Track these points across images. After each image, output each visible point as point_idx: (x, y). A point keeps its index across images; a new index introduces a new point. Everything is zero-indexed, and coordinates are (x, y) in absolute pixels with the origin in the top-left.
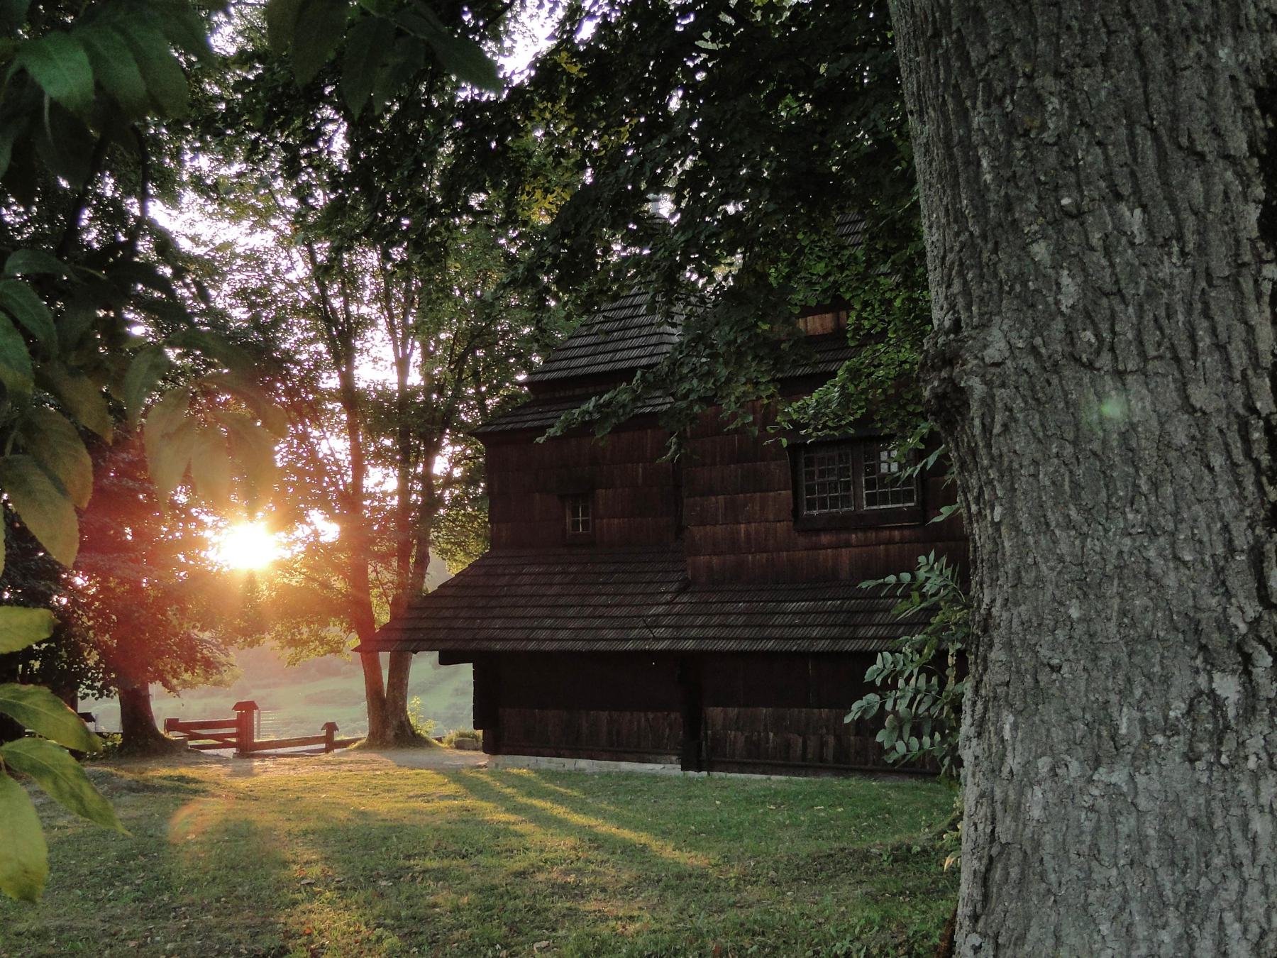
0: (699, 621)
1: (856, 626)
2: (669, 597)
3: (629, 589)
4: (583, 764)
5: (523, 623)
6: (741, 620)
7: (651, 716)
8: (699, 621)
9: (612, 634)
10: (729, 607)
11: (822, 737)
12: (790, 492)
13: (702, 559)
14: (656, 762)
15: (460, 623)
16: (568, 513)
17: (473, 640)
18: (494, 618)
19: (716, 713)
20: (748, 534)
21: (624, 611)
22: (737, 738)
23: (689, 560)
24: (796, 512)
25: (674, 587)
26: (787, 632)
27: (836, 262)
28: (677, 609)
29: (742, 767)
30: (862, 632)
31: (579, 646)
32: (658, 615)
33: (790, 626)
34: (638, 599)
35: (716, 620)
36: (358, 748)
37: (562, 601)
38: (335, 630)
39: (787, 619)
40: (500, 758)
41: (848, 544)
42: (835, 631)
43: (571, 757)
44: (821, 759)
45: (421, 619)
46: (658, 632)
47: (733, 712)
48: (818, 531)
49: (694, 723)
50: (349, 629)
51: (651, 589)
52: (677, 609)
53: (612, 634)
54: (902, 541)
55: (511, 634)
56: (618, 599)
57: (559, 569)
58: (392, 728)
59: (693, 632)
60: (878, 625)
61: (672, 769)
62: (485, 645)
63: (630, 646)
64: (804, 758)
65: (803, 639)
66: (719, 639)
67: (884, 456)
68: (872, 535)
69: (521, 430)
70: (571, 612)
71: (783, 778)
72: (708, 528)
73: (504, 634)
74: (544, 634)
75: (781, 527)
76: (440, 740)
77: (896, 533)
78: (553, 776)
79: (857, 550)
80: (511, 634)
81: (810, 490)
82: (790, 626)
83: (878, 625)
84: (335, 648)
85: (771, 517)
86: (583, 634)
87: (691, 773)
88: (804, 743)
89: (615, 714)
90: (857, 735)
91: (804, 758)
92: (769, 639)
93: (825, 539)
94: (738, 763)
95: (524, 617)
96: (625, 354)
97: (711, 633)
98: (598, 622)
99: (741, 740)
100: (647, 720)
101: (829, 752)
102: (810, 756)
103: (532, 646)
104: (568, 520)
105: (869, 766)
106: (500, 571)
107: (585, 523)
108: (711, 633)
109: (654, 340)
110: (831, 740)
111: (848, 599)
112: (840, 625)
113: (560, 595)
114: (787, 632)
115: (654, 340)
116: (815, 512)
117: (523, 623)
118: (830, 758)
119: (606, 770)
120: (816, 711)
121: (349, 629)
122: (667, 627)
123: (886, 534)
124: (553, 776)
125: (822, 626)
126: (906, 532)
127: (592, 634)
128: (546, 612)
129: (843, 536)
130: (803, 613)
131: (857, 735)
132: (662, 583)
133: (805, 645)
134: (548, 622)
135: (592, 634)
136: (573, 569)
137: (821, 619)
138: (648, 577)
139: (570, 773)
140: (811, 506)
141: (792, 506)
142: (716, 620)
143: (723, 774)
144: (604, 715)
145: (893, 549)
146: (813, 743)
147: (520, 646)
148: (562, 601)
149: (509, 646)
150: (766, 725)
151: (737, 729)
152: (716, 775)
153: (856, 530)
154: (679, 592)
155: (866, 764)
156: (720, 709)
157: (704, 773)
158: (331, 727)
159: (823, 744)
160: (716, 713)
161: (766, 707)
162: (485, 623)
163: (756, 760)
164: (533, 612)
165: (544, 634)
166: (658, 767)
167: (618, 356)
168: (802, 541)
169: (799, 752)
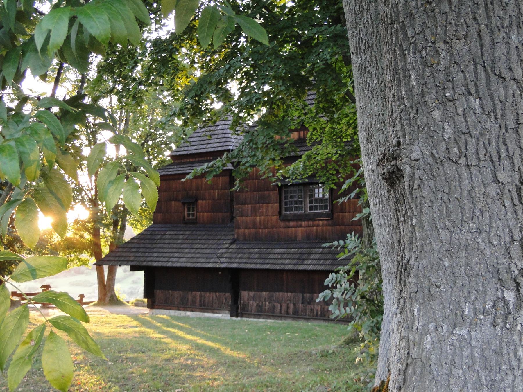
0: (240, 256)
1: (304, 259)
2: (227, 246)
3: (211, 242)
4: (189, 313)
5: (167, 255)
6: (257, 256)
7: (218, 294)
8: (240, 256)
9: (203, 260)
10: (252, 251)
11: (288, 304)
12: (278, 204)
13: (241, 231)
14: (219, 313)
15: (139, 254)
16: (186, 209)
17: (145, 261)
18: (154, 252)
19: (244, 294)
20: (260, 221)
21: (208, 251)
22: (253, 304)
23: (236, 231)
24: (280, 213)
25: (229, 242)
26: (275, 261)
27: (303, 112)
28: (230, 250)
29: (255, 316)
30: (306, 262)
31: (189, 265)
32: (223, 253)
33: (277, 259)
34: (214, 246)
35: (246, 256)
36: (94, 305)
37: (182, 246)
38: (85, 256)
39: (275, 256)
40: (155, 311)
41: (301, 226)
42: (295, 261)
43: (184, 310)
44: (287, 313)
45: (123, 252)
46: (222, 260)
47: (252, 293)
48: (289, 220)
49: (236, 298)
50: (91, 255)
51: (221, 242)
52: (230, 250)
53: (203, 260)
54: (323, 226)
55: (160, 259)
56: (206, 246)
57: (181, 233)
58: (108, 297)
59: (237, 260)
60: (312, 259)
61: (224, 316)
62: (150, 264)
63: (210, 265)
64: (280, 313)
65: (282, 264)
66: (247, 263)
67: (317, 191)
68: (311, 223)
69: (167, 175)
70: (186, 251)
71: (273, 321)
72: (244, 218)
73: (158, 259)
74: (175, 260)
75: (274, 218)
76: (128, 302)
77: (321, 222)
78: (177, 318)
79: (305, 229)
80: (160, 259)
81: (286, 204)
82: (277, 259)
83: (312, 259)
84: (84, 263)
85: (270, 214)
86: (191, 260)
87: (234, 318)
88: (281, 306)
89: (203, 293)
90: (302, 303)
91: (280, 313)
92: (268, 264)
93: (292, 224)
95: (166, 253)
96: (212, 145)
97: (244, 261)
98: (198, 255)
99: (255, 305)
100: (216, 295)
101: (291, 311)
102: (283, 312)
103: (169, 264)
104: (186, 213)
105: (307, 317)
106: (157, 233)
107: (193, 215)
108: (244, 261)
109: (224, 140)
110: (292, 306)
111: (300, 248)
112: (297, 259)
113: (181, 244)
114: (275, 261)
115: (224, 140)
116: (288, 213)
117: (167, 255)
118: (291, 313)
119: (198, 316)
120: (286, 293)
121: (91, 255)
122: (226, 258)
123: (317, 222)
124: (177, 318)
125: (290, 259)
126: (325, 222)
127: (194, 260)
128: (175, 250)
129: (299, 223)
130: (282, 254)
131: (302, 303)
132: (225, 240)
133: (282, 267)
134: (176, 255)
135: (194, 260)
136: (187, 233)
137: (289, 256)
138: (219, 237)
139: (184, 317)
140: (286, 210)
141: (278, 210)
142: (246, 256)
143: (247, 319)
144: (198, 293)
145: (319, 228)
146: (284, 306)
147: (165, 264)
148: (182, 246)
149: (159, 264)
150: (265, 299)
151: (254, 301)
152: (245, 319)
153: (304, 220)
154: (232, 244)
155: (306, 315)
156: (247, 292)
157: (239, 318)
158: (82, 296)
159: (288, 308)
160: (244, 294)
161: (266, 291)
162: (150, 254)
163: (260, 313)
164: (171, 250)
165: (175, 260)
167: (209, 146)
168: (282, 224)
169: (278, 311)
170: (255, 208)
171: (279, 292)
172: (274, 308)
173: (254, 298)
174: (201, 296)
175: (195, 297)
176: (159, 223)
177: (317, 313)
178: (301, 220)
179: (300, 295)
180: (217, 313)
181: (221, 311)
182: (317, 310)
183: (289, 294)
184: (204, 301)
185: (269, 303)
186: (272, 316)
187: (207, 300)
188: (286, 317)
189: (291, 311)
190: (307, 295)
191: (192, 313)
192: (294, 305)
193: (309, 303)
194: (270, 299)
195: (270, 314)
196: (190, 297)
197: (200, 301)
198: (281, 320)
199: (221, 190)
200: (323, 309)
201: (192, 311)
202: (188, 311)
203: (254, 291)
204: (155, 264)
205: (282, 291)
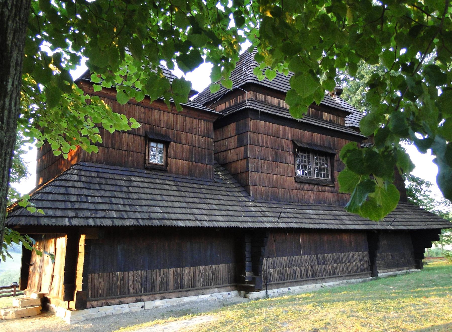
4: (159, 303)
7: (201, 268)
22: (274, 272)
29: (279, 285)
43: (149, 300)
64: (302, 278)
71: (298, 287)
90: (318, 264)
91: (302, 278)
94: (277, 284)
101: (310, 274)
110: (309, 268)
126: (329, 188)
131: (318, 264)
143: (314, 285)
144: (171, 271)
146: (303, 269)
150: (286, 265)
160: (267, 261)
161: (285, 256)
166: (207, 296)
168: (297, 185)
170: (271, 164)
171: (297, 255)
172: (295, 272)
173: (274, 265)
174: (177, 274)
175: (166, 275)
176: (97, 162)
177: (330, 272)
178: (314, 184)
179: (314, 256)
180: (203, 294)
181: (208, 291)
182: (330, 269)
183: (306, 256)
184: (181, 281)
185: (290, 268)
186: (295, 282)
187: (186, 278)
188: (307, 280)
189: (310, 274)
190: (320, 256)
191: (164, 301)
192: (312, 267)
193: (324, 263)
194: (291, 264)
195: (292, 280)
196: (157, 278)
197: (176, 281)
198: (303, 285)
199: (203, 136)
200: (334, 267)
201: (164, 298)
202: (155, 299)
203: (274, 257)
204: (181, 224)
205: (300, 255)
